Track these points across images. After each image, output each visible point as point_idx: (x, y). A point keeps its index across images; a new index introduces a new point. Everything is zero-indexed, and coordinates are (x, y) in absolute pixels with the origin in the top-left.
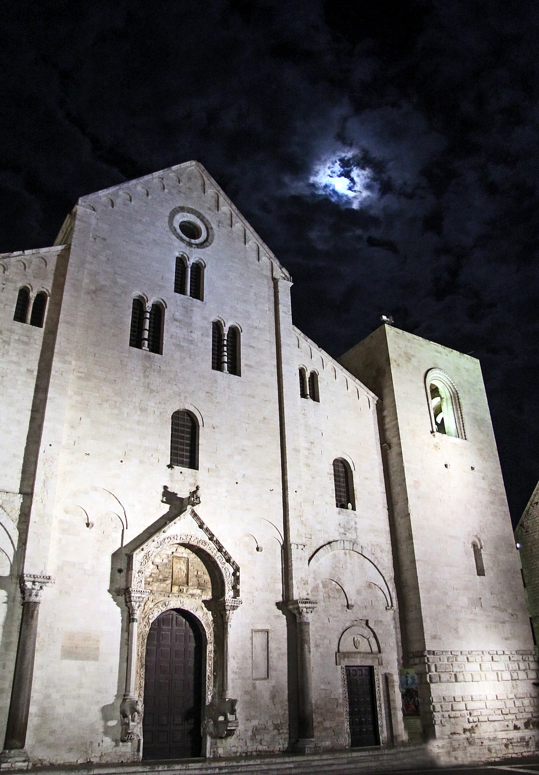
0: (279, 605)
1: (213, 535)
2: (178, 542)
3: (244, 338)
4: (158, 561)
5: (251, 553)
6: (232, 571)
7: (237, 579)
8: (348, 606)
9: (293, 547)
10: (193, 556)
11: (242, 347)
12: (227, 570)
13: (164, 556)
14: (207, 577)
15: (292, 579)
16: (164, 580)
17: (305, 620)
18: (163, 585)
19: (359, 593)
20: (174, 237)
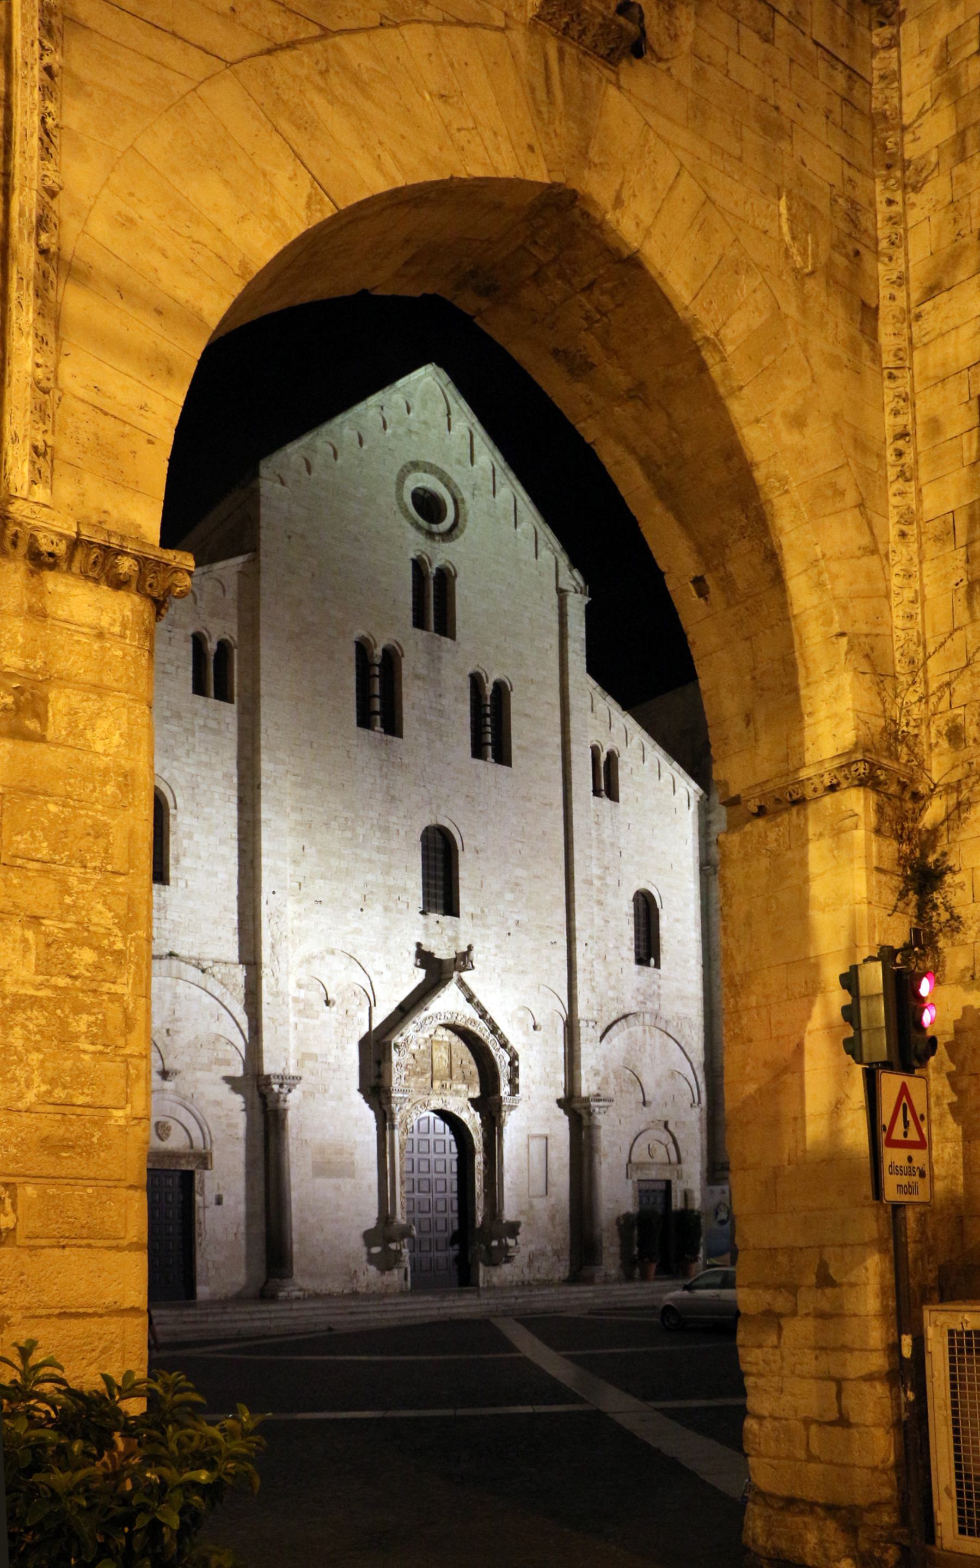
0: (560, 1103)
1: (486, 1012)
2: (442, 1022)
3: (517, 703)
4: (413, 1047)
5: (526, 1033)
6: (507, 1059)
7: (515, 1071)
8: (644, 1103)
9: (582, 1024)
10: (455, 1040)
11: (513, 716)
12: (502, 1058)
13: (421, 1041)
14: (474, 1068)
15: (579, 1067)
16: (422, 1073)
17: (597, 1123)
18: (422, 1080)
19: (658, 1084)
20: (406, 524)
